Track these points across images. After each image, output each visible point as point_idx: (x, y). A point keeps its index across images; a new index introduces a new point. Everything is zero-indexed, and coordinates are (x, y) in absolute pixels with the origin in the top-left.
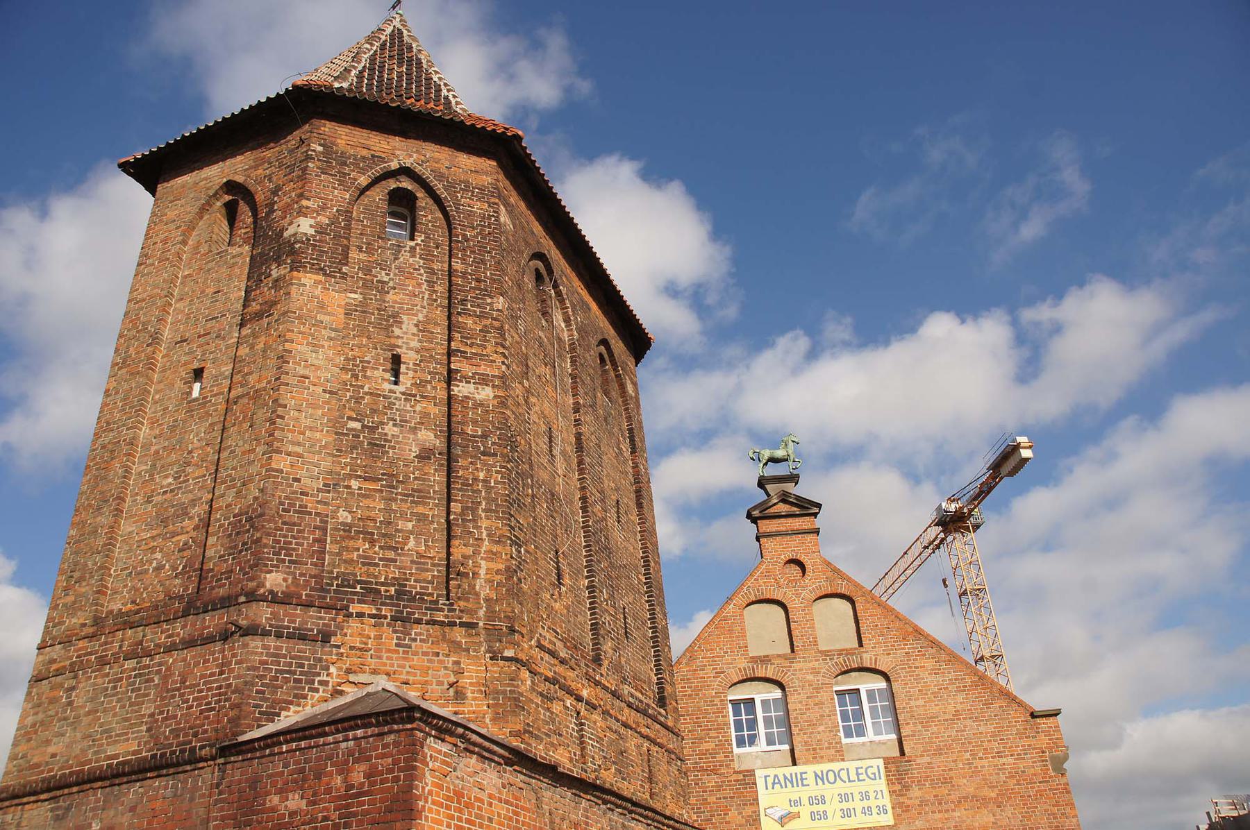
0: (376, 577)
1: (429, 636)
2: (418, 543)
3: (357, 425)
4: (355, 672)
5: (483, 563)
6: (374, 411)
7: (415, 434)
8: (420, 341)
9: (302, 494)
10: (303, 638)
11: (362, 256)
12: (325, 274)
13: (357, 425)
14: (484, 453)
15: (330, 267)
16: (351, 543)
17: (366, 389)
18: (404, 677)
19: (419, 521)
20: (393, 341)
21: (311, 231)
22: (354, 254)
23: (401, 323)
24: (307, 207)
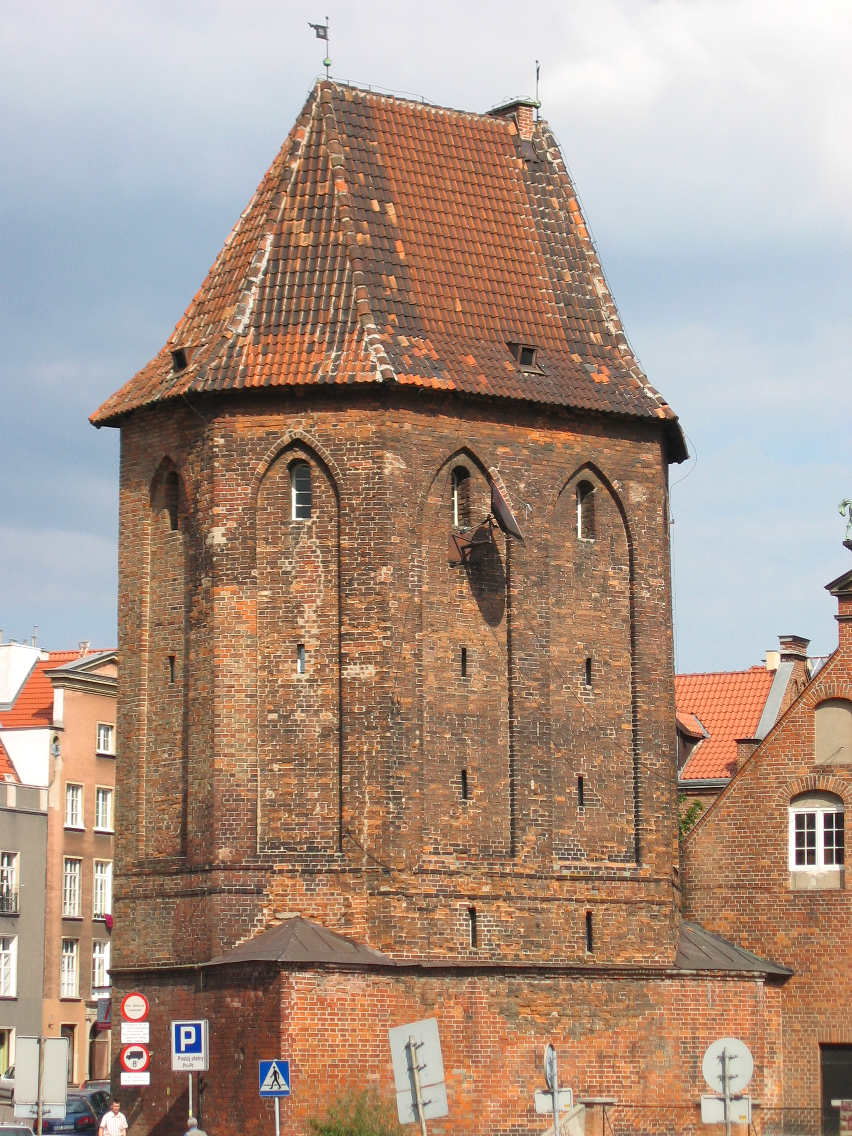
0: (294, 839)
1: (328, 881)
2: (323, 809)
3: (274, 717)
4: (279, 912)
5: (366, 821)
6: (287, 701)
7: (318, 716)
8: (319, 627)
9: (238, 786)
10: (245, 892)
11: (270, 549)
12: (240, 583)
13: (274, 717)
14: (368, 728)
15: (241, 574)
16: (276, 815)
17: (280, 683)
18: (311, 912)
19: (323, 790)
20: (299, 632)
21: (223, 541)
22: (262, 549)
23: (303, 612)
24: (219, 515)
